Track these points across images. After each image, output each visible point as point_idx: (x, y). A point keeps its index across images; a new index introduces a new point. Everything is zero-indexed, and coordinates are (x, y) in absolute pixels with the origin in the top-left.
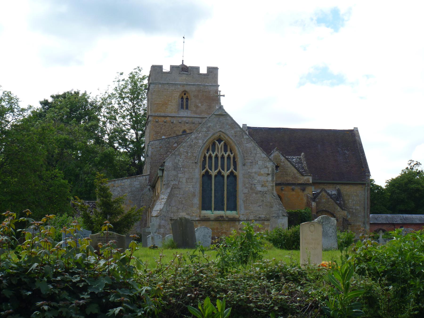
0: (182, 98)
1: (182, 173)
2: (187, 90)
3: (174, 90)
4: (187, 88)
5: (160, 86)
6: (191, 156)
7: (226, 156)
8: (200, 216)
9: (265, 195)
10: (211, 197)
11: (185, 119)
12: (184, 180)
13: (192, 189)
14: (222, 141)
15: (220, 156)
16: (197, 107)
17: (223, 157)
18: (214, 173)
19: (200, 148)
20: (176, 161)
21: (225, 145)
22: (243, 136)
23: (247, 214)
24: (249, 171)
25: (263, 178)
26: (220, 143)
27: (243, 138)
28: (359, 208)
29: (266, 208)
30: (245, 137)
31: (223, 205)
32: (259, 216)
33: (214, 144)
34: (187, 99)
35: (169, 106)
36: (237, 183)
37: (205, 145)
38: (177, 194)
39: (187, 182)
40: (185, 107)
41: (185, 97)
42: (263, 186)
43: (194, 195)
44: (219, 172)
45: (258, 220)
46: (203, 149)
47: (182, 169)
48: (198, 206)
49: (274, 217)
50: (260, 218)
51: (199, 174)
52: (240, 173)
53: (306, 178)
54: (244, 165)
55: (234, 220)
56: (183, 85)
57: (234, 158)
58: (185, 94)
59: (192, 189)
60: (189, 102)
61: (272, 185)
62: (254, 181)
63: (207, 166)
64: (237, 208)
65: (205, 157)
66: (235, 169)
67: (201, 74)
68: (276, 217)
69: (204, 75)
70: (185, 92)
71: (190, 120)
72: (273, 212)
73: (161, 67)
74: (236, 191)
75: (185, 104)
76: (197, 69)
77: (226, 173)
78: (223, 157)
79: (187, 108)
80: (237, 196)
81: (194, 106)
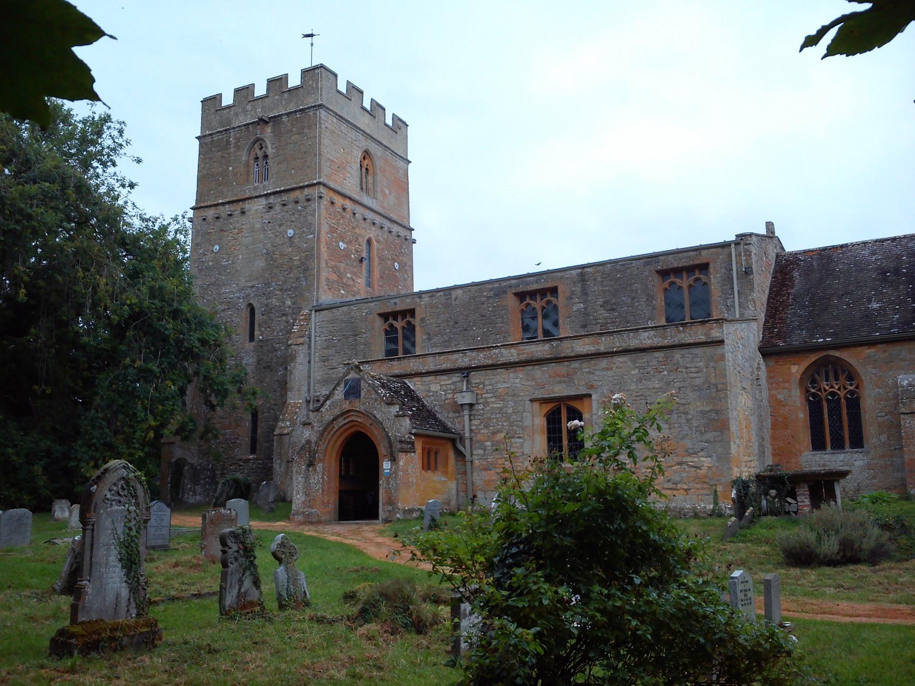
2: (372, 151)
5: (335, 120)
11: (370, 215)
16: (383, 192)
35: (349, 175)
60: (370, 178)
71: (378, 220)
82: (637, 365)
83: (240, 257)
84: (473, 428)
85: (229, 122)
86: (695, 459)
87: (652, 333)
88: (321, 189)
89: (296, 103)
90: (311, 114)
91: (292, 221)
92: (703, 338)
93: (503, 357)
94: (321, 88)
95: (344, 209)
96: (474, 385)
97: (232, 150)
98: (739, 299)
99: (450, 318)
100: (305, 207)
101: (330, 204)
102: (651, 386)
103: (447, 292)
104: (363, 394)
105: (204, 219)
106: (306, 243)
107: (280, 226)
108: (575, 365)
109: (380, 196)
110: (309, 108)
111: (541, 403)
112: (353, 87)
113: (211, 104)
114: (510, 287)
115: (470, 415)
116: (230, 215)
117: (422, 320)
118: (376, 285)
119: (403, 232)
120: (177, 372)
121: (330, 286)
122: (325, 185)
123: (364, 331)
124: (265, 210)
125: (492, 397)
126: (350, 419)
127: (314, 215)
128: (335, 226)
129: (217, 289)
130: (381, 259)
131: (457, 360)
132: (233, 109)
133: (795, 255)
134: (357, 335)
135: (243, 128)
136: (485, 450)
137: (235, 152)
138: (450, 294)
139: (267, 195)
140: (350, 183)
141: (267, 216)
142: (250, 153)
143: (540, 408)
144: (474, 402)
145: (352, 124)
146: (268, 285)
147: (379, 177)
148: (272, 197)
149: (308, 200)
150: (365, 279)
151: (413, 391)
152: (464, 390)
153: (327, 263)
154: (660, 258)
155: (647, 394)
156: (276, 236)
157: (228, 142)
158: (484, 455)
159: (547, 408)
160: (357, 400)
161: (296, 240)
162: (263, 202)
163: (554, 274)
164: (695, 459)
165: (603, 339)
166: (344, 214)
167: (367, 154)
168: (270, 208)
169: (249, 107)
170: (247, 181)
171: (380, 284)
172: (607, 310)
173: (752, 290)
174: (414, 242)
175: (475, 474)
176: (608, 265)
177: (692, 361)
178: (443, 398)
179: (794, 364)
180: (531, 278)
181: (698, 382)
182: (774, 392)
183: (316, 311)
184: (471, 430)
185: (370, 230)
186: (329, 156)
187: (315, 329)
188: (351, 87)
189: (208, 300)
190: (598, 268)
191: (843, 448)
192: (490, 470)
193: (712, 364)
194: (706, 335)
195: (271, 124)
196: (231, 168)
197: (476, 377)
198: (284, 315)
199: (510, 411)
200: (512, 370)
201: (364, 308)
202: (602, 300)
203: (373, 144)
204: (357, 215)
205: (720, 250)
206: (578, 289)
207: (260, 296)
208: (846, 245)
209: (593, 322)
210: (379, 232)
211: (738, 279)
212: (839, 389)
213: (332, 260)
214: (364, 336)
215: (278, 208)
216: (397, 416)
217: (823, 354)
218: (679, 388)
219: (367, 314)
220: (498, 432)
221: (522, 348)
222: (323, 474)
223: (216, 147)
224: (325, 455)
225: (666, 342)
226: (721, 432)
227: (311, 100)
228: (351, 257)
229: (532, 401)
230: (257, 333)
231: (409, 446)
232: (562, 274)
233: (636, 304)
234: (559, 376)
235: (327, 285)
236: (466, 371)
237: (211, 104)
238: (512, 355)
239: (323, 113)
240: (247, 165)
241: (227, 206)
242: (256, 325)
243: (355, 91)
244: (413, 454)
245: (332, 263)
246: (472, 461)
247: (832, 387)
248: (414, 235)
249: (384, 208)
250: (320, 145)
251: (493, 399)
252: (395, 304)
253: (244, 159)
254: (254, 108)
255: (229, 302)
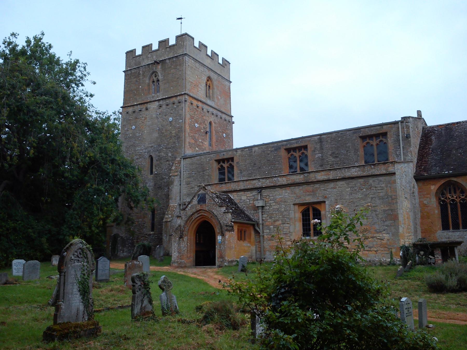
5: (193, 62)
11: (211, 110)
16: (218, 99)
35: (200, 89)
60: (211, 91)
71: (215, 112)
82: (349, 186)
83: (146, 132)
84: (264, 218)
85: (140, 63)
86: (381, 235)
87: (357, 169)
88: (186, 97)
89: (173, 53)
90: (181, 58)
91: (171, 113)
92: (384, 172)
93: (279, 182)
94: (186, 45)
95: (198, 107)
96: (264, 197)
97: (141, 77)
98: (403, 151)
99: (252, 162)
100: (178, 106)
101: (190, 104)
102: (357, 197)
103: (250, 149)
104: (207, 201)
105: (127, 113)
106: (179, 124)
107: (165, 116)
108: (317, 186)
109: (216, 101)
110: (179, 56)
111: (299, 206)
112: (202, 44)
113: (130, 54)
114: (283, 145)
115: (262, 212)
116: (140, 110)
117: (237, 163)
118: (214, 145)
119: (227, 118)
120: (114, 191)
121: (191, 146)
122: (188, 95)
123: (208, 169)
124: (158, 108)
125: (273, 203)
126: (200, 214)
127: (182, 110)
128: (193, 115)
129: (134, 148)
130: (217, 132)
131: (255, 183)
132: (141, 56)
133: (432, 127)
134: (204, 171)
135: (147, 66)
136: (270, 230)
137: (143, 78)
138: (252, 150)
139: (159, 100)
140: (201, 93)
141: (159, 111)
142: (150, 79)
143: (299, 208)
144: (265, 205)
145: (201, 63)
146: (159, 146)
147: (215, 90)
148: (161, 101)
149: (179, 102)
150: (208, 142)
151: (233, 200)
152: (259, 199)
153: (189, 134)
154: (361, 130)
155: (355, 201)
156: (163, 121)
157: (139, 73)
158: (269, 233)
159: (302, 208)
160: (204, 205)
161: (173, 123)
162: (157, 103)
163: (306, 139)
164: (381, 235)
165: (332, 172)
166: (198, 109)
167: (209, 79)
168: (161, 106)
169: (149, 56)
170: (149, 93)
171: (216, 144)
172: (334, 157)
173: (410, 146)
174: (233, 123)
175: (265, 242)
176: (334, 134)
177: (378, 184)
178: (248, 203)
179: (433, 185)
180: (294, 141)
181: (381, 194)
182: (422, 199)
183: (184, 159)
184: (263, 220)
185: (211, 117)
186: (190, 80)
187: (183, 168)
188: (201, 44)
189: (130, 154)
190: (329, 135)
191: (459, 229)
192: (273, 240)
193: (389, 185)
194: (386, 170)
195: (160, 64)
196: (140, 87)
197: (265, 193)
198: (167, 161)
199: (283, 210)
200: (284, 189)
201: (208, 157)
202: (331, 152)
203: (213, 73)
204: (204, 110)
205: (393, 125)
206: (318, 146)
207: (156, 151)
208: (460, 122)
209: (326, 163)
210: (216, 118)
211: (402, 140)
212: (456, 198)
213: (192, 133)
214: (208, 171)
215: (164, 107)
216: (224, 213)
217: (448, 179)
218: (372, 198)
219: (209, 160)
220: (278, 220)
221: (289, 177)
222: (187, 242)
223: (133, 76)
224: (188, 233)
225: (365, 174)
226: (394, 221)
227: (181, 52)
228: (201, 131)
229: (294, 204)
230: (154, 170)
231: (231, 228)
232: (309, 139)
233: (349, 154)
234: (308, 192)
235: (189, 145)
236: (260, 189)
237: (130, 54)
238: (284, 181)
239: (187, 58)
240: (149, 85)
241: (139, 106)
242: (154, 166)
243: (203, 46)
244: (233, 232)
245: (192, 134)
246: (263, 236)
247: (453, 197)
248: (234, 120)
250: (185, 74)
251: (274, 204)
252: (224, 155)
253: (147, 82)
254: (152, 56)
255: (140, 155)
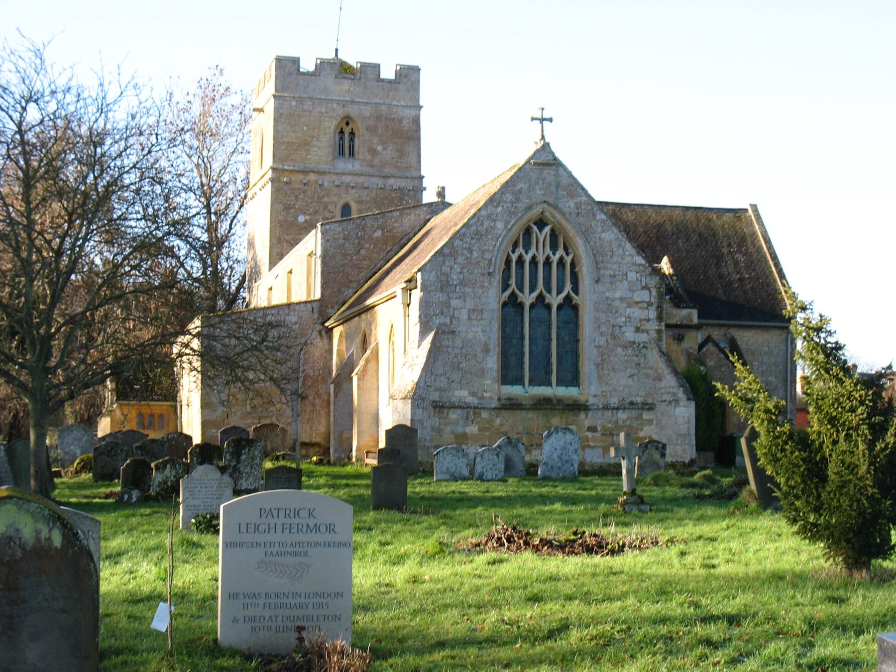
0: (342, 132)
1: (460, 298)
2: (352, 115)
3: (325, 115)
4: (353, 111)
6: (477, 257)
7: (555, 259)
8: (499, 399)
9: (643, 351)
10: (523, 354)
11: (348, 179)
12: (464, 315)
13: (481, 336)
14: (546, 225)
15: (541, 259)
16: (373, 152)
17: (548, 263)
18: (527, 298)
19: (500, 239)
20: (446, 269)
21: (554, 235)
22: (594, 215)
23: (604, 394)
24: (607, 294)
25: (637, 313)
26: (541, 229)
27: (595, 219)
28: (774, 380)
29: (646, 381)
30: (598, 217)
31: (549, 372)
32: (630, 399)
33: (528, 232)
34: (352, 133)
35: (314, 149)
36: (580, 322)
37: (511, 234)
38: (448, 347)
39: (469, 318)
40: (347, 151)
41: (347, 130)
42: (638, 330)
43: (487, 351)
44: (541, 297)
45: (629, 409)
46: (505, 242)
47: (458, 288)
48: (495, 374)
49: (665, 401)
50: (632, 403)
51: (497, 300)
52: (586, 300)
53: (685, 312)
54: (597, 281)
55: (577, 407)
56: (344, 104)
57: (573, 265)
58: (347, 124)
59: (481, 336)
60: (356, 140)
61: (657, 328)
62: (619, 319)
63: (513, 281)
64: (581, 381)
65: (508, 261)
66: (576, 289)
67: (383, 80)
68: (670, 402)
69: (390, 82)
70: (348, 121)
71: (361, 180)
72: (663, 391)
73: (296, 61)
74: (577, 341)
75: (347, 145)
76: (376, 67)
77: (555, 300)
78: (548, 263)
79: (352, 153)
80: (580, 351)
81: (369, 151)
166: (306, 188)
210: (364, 194)
249: (372, 166)
